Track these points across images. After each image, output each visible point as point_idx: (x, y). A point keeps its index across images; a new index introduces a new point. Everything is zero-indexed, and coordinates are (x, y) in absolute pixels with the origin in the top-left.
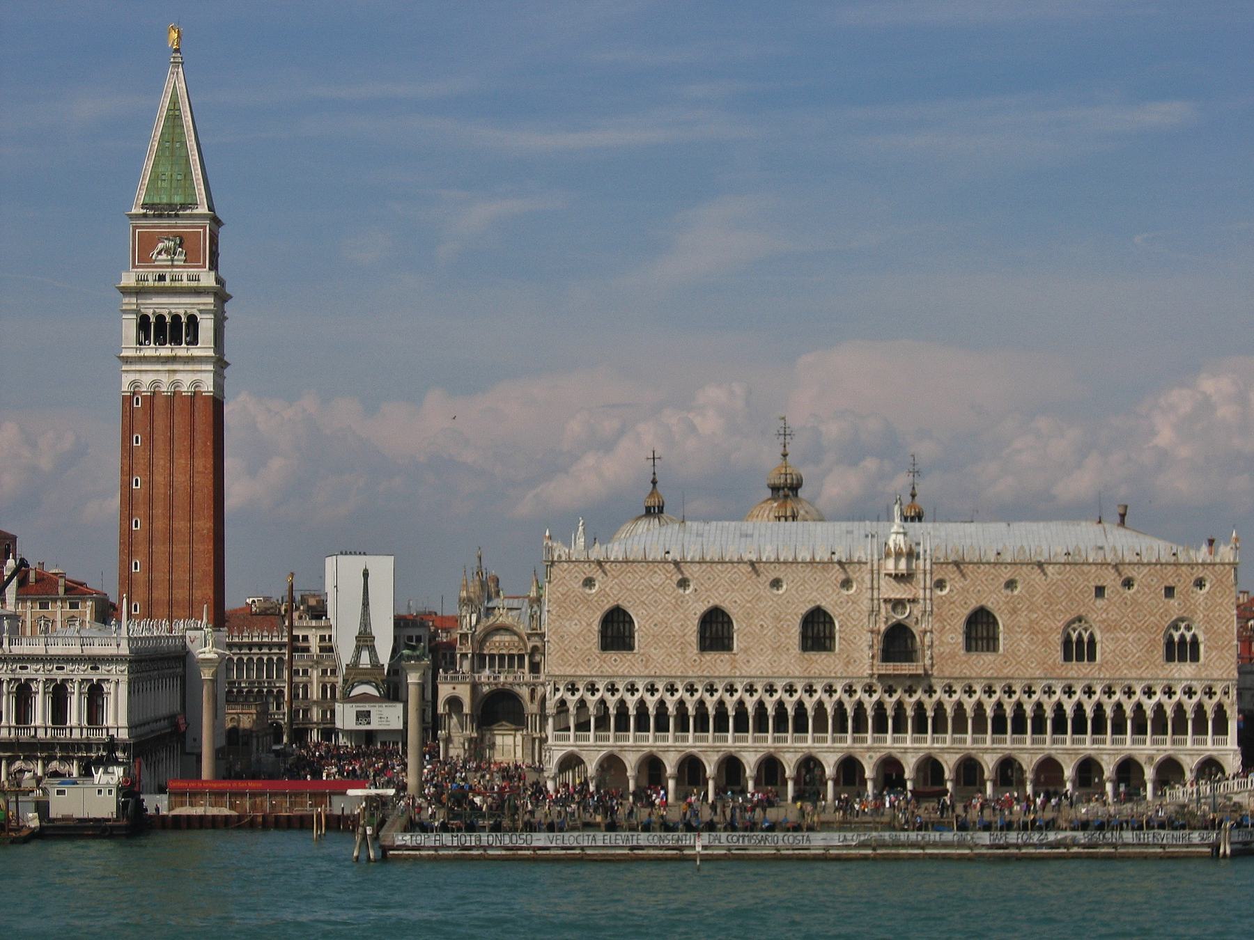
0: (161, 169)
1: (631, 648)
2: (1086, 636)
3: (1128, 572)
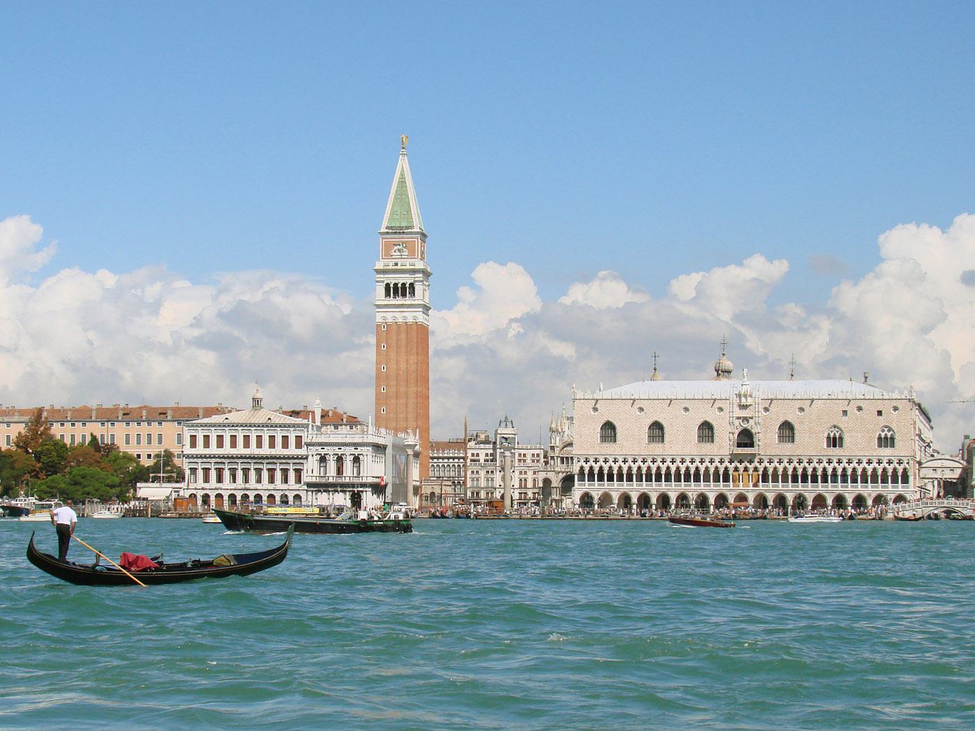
3: (861, 404)
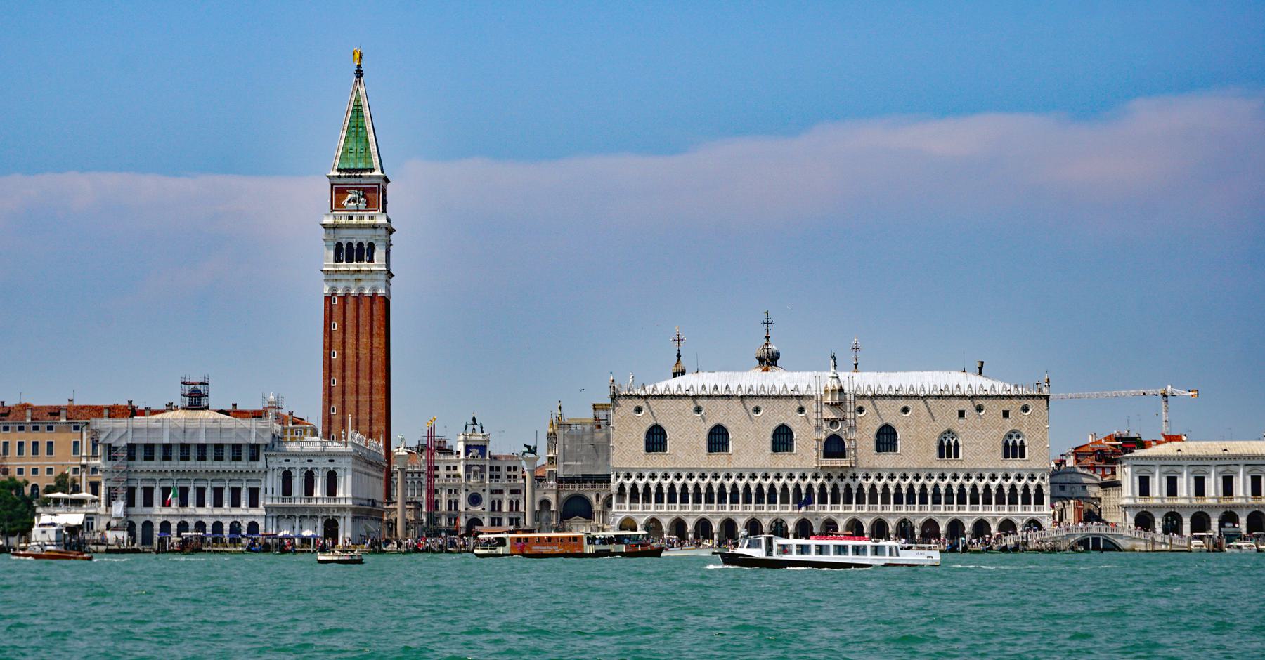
0: (349, 145)
1: (665, 450)
2: (953, 442)
